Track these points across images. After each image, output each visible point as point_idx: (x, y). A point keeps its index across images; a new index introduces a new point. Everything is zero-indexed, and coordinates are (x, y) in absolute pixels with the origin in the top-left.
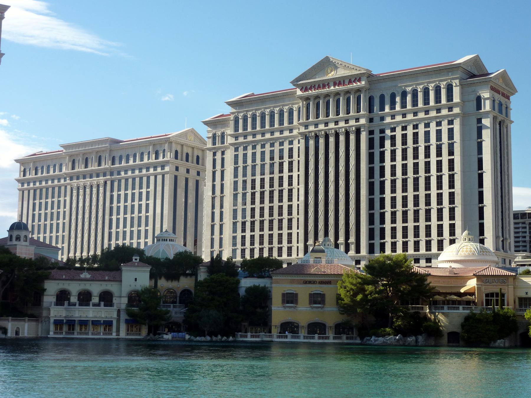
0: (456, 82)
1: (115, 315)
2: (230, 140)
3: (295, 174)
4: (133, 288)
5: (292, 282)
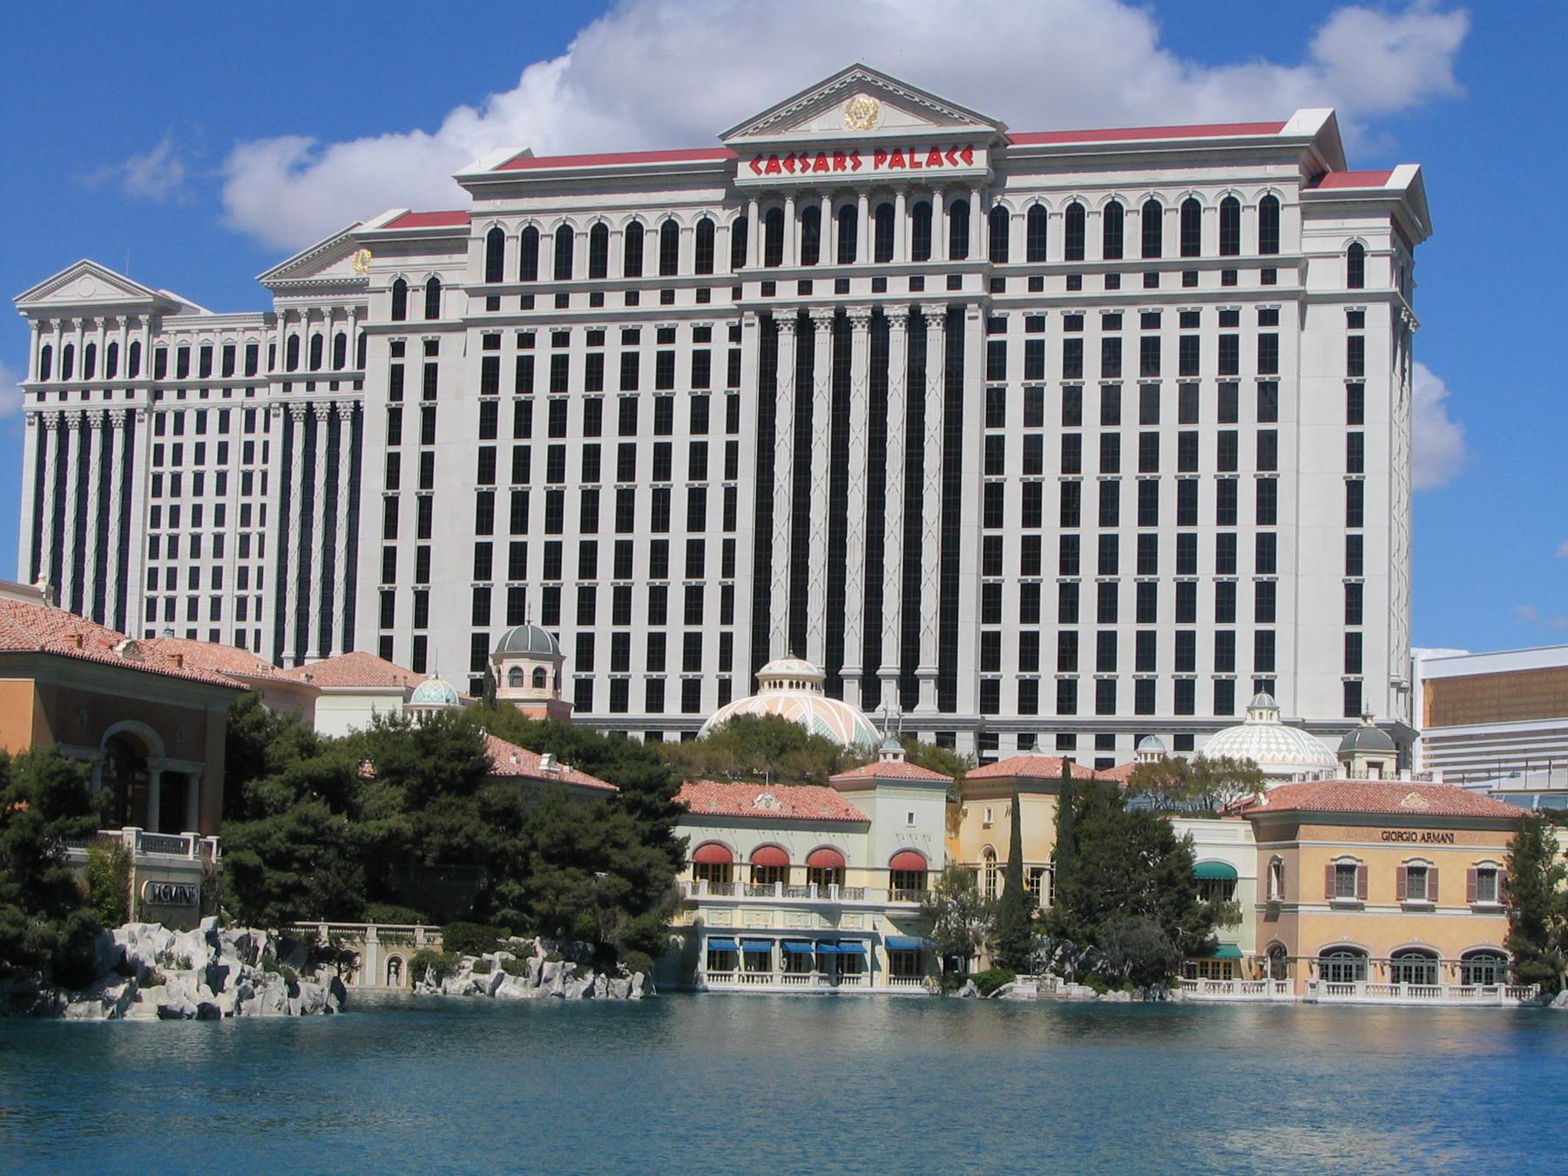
0: (1289, 195)
2: (453, 307)
3: (716, 439)
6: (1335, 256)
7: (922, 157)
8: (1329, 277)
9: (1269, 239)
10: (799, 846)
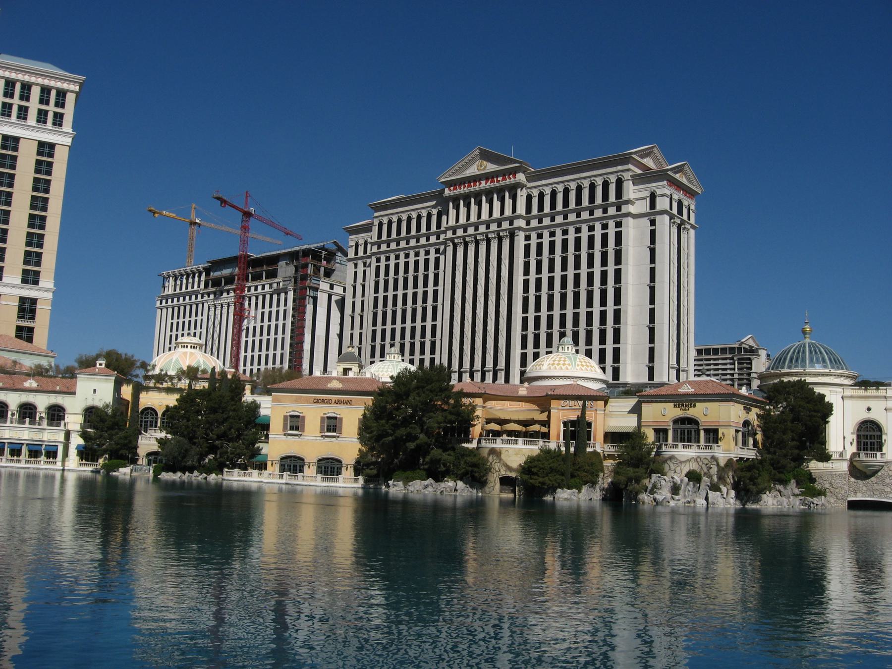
1: (61, 438)
4: (90, 403)
5: (297, 401)
6: (645, 198)
7: (500, 179)
8: (642, 207)
9: (619, 194)
10: (42, 402)
